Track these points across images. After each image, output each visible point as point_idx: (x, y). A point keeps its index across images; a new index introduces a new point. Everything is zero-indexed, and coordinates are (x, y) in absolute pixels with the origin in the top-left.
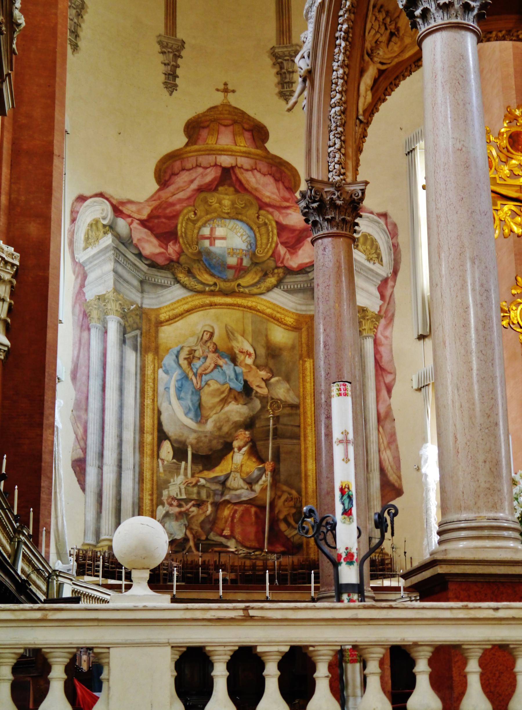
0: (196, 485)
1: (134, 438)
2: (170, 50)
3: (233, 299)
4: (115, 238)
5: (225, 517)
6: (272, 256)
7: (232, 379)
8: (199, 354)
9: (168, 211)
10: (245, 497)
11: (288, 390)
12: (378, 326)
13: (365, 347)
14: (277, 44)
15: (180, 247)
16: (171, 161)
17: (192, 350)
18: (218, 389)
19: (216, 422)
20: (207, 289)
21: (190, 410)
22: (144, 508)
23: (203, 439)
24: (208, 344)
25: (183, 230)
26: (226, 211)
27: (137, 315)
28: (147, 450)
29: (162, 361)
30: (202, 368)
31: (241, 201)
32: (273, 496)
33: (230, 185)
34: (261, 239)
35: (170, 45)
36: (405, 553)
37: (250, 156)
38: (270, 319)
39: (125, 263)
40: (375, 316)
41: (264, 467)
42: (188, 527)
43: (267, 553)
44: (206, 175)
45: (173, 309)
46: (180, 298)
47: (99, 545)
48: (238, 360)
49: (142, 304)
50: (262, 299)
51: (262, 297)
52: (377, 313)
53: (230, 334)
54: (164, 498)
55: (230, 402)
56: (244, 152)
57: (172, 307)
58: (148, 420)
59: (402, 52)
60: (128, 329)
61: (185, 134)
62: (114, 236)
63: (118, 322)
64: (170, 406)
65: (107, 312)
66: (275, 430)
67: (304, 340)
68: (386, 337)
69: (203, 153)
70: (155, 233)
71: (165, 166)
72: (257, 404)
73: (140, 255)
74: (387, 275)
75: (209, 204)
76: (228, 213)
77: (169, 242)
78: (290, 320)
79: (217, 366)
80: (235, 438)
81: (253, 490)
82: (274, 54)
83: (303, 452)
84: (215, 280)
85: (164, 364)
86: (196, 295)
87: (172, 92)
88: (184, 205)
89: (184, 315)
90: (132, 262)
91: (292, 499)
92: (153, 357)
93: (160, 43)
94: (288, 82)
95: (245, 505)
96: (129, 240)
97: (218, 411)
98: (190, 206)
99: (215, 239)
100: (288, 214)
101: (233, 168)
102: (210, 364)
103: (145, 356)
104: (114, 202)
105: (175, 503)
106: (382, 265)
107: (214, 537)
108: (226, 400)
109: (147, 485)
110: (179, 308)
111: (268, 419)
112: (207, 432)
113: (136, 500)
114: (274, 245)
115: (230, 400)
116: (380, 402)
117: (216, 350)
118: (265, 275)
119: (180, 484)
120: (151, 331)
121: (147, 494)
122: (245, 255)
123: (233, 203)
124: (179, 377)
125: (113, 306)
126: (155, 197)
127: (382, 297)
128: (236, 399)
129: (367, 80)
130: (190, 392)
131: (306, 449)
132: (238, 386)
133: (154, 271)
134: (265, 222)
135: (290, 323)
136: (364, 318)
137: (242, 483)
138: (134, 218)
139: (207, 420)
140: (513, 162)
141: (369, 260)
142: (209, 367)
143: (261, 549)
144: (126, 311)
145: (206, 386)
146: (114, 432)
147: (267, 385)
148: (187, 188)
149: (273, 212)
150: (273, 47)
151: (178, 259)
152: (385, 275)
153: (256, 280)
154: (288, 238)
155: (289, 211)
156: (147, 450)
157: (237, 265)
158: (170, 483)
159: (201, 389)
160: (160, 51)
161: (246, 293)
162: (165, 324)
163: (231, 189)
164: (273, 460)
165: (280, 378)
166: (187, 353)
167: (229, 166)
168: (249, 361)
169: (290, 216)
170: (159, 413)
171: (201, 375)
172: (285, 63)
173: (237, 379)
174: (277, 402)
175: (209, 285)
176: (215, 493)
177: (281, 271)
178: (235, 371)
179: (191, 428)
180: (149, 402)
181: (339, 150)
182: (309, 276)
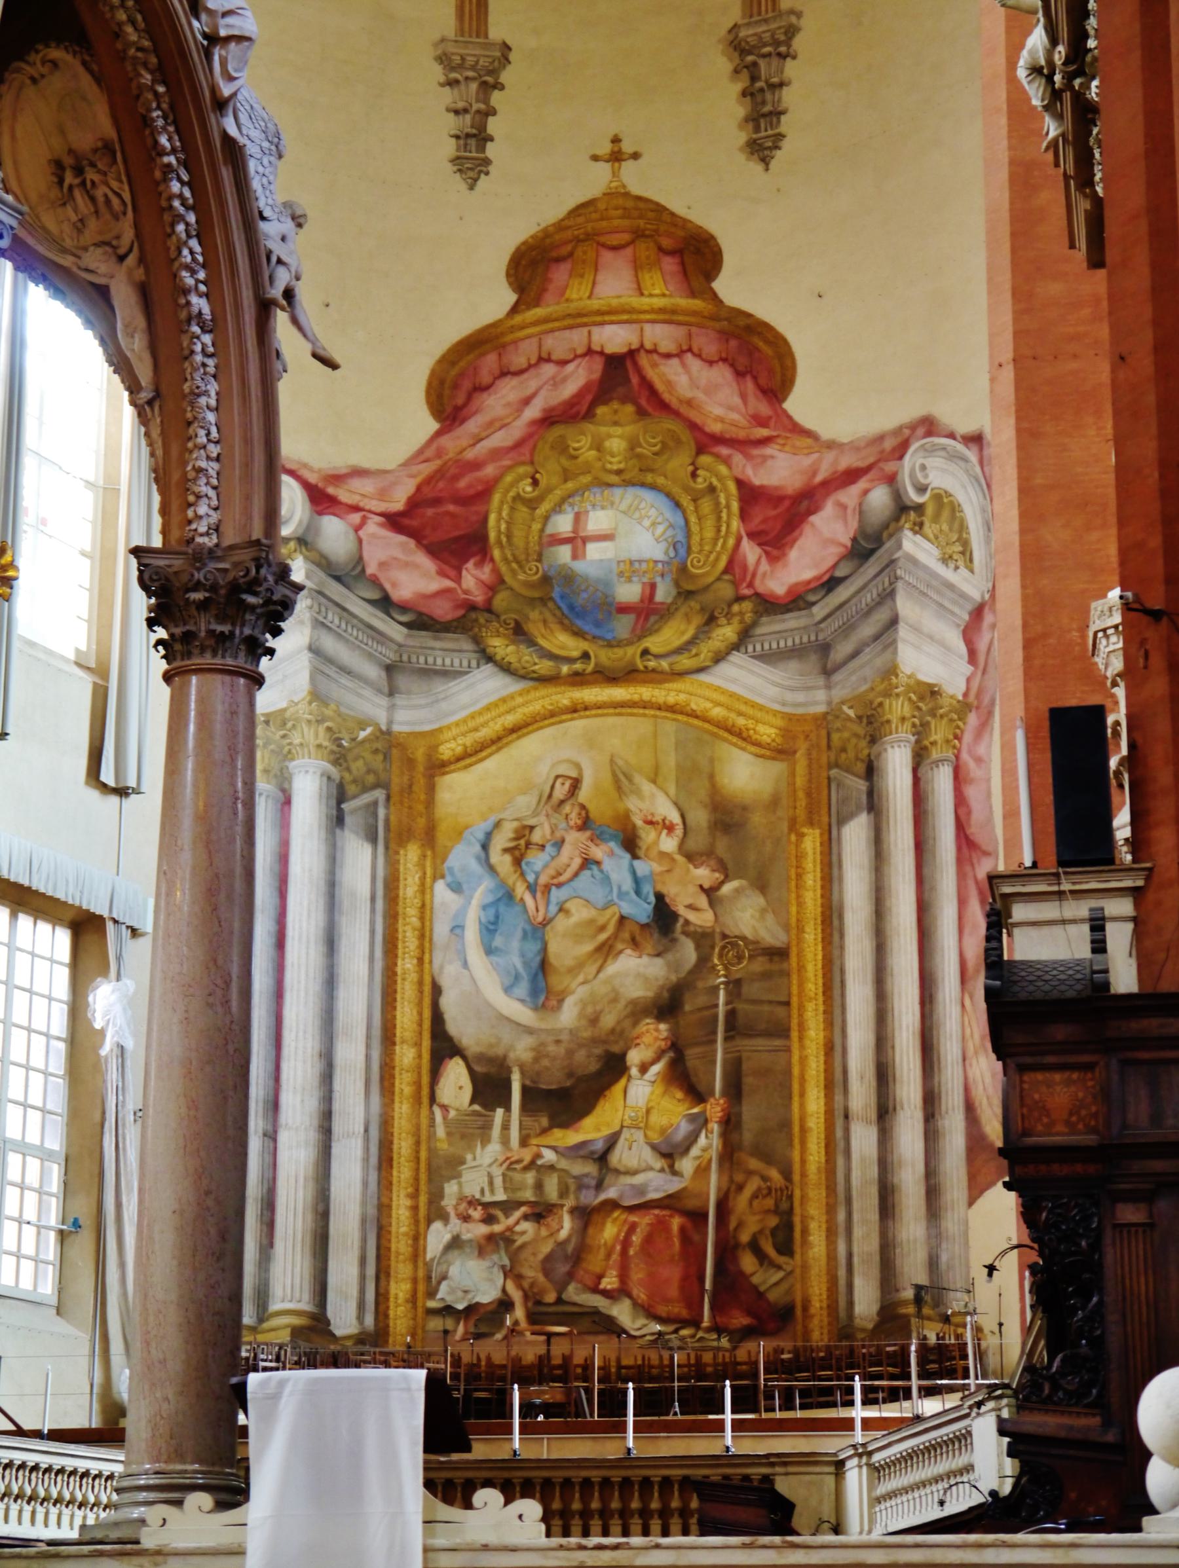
0: (532, 1165)
1: (368, 1057)
2: (471, 74)
3: (632, 690)
4: (314, 568)
5: (605, 1244)
7: (627, 893)
8: (544, 836)
9: (462, 484)
10: (656, 1190)
11: (763, 911)
12: (962, 732)
13: (936, 786)
14: (743, 17)
15: (496, 571)
16: (471, 357)
17: (525, 827)
18: (591, 922)
19: (584, 1004)
20: (565, 669)
21: (517, 977)
22: (394, 1229)
23: (552, 1048)
24: (567, 808)
25: (503, 526)
26: (615, 467)
27: (376, 751)
28: (404, 1084)
29: (443, 862)
30: (552, 872)
31: (654, 438)
32: (725, 1186)
33: (624, 400)
34: (701, 529)
35: (470, 60)
36: (1001, 1325)
37: (675, 318)
38: (722, 733)
39: (343, 626)
40: (957, 706)
41: (704, 1112)
42: (509, 1273)
43: (708, 1330)
44: (564, 380)
45: (476, 730)
46: (493, 698)
47: (266, 1325)
48: (641, 844)
49: (390, 722)
50: (701, 684)
51: (703, 677)
52: (961, 698)
53: (621, 781)
54: (449, 1202)
55: (621, 952)
56: (662, 310)
57: (471, 724)
58: (407, 1009)
60: (351, 789)
61: (510, 284)
62: (313, 562)
63: (322, 775)
64: (465, 972)
65: (289, 752)
66: (731, 1015)
67: (800, 781)
68: (979, 760)
69: (557, 324)
70: (425, 542)
71: (454, 372)
72: (688, 953)
73: (385, 603)
74: (983, 597)
75: (572, 452)
76: (619, 472)
77: (466, 561)
78: (767, 732)
79: (588, 863)
80: (631, 1043)
81: (675, 1173)
82: (738, 46)
83: (796, 1071)
84: (585, 645)
85: (450, 869)
86: (536, 689)
87: (476, 180)
88: (507, 462)
89: (505, 741)
90: (361, 621)
91: (769, 1189)
92: (419, 852)
93: (443, 59)
94: (771, 113)
95: (656, 1212)
96: (354, 568)
97: (590, 977)
98: (523, 463)
99: (585, 540)
100: (765, 458)
101: (632, 354)
102: (572, 859)
103: (397, 853)
104: (312, 478)
105: (477, 1214)
106: (972, 571)
108: (611, 947)
109: (402, 1172)
110: (491, 724)
112: (561, 1031)
113: (372, 1211)
114: (731, 542)
115: (620, 946)
116: (967, 931)
117: (585, 824)
118: (711, 620)
119: (490, 1165)
120: (415, 788)
121: (403, 1193)
122: (662, 575)
123: (633, 444)
124: (490, 899)
125: (309, 735)
126: (429, 453)
128: (635, 943)
131: (803, 1060)
132: (642, 911)
133: (424, 638)
134: (711, 483)
135: (769, 741)
137: (648, 1156)
138: (370, 511)
139: (561, 1001)
141: (946, 560)
142: (569, 866)
143: (696, 1323)
144: (345, 743)
145: (561, 916)
146: (309, 1045)
147: (712, 904)
148: (514, 420)
149: (730, 456)
150: (735, 25)
151: (489, 601)
153: (687, 636)
154: (765, 521)
155: (769, 451)
156: (404, 1084)
157: (642, 601)
158: (463, 1162)
159: (546, 923)
160: (442, 79)
161: (662, 672)
162: (453, 767)
163: (629, 409)
164: (725, 1093)
165: (744, 882)
166: (512, 835)
167: (625, 350)
168: (669, 844)
169: (769, 463)
170: (437, 990)
171: (547, 888)
172: (762, 64)
173: (638, 892)
174: (734, 945)
175: (570, 660)
177: (747, 606)
178: (634, 873)
179: (518, 1024)
180: (408, 966)
182: (812, 615)
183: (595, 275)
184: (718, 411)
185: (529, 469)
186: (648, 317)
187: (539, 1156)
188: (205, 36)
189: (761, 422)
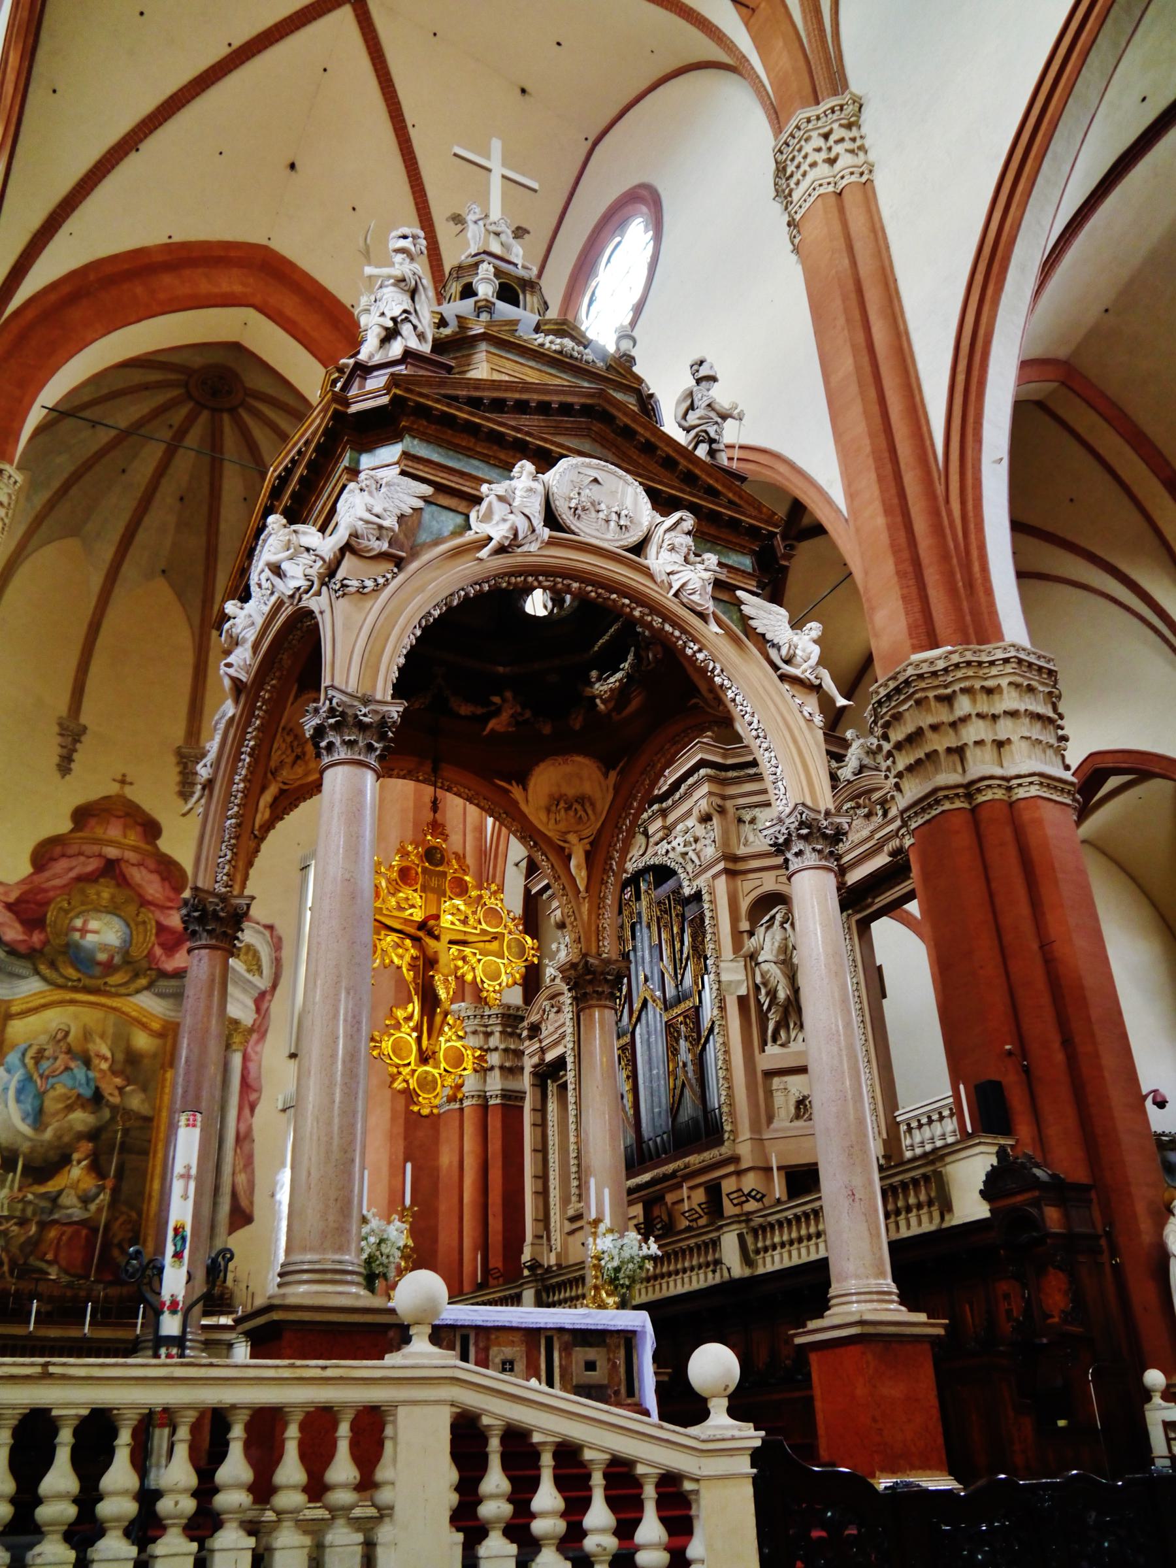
0: (22, 1200)
6: (146, 956)
9: (39, 897)
11: (143, 1101)
15: (47, 936)
18: (65, 1094)
20: (70, 984)
21: (28, 1115)
24: (62, 1044)
33: (112, 878)
51: (131, 999)
53: (87, 1035)
59: (307, 774)
66: (123, 1144)
68: (256, 1053)
72: (107, 1114)
78: (156, 1026)
80: (76, 1150)
81: (87, 1209)
83: (150, 1171)
93: (60, 725)
100: (170, 915)
101: (118, 861)
107: (34, 1262)
111: (116, 1132)
117: (69, 1051)
118: (136, 976)
123: (113, 897)
124: (22, 1078)
127: (258, 1011)
128: (83, 1107)
129: (267, 798)
130: (31, 1095)
131: (154, 1166)
132: (87, 1092)
133: (12, 959)
136: (235, 1030)
139: (46, 1128)
140: (401, 895)
141: (249, 971)
143: (87, 1277)
151: (42, 949)
152: (263, 988)
155: (172, 912)
159: (44, 1093)
163: (113, 882)
164: (115, 1177)
168: (104, 1066)
171: (47, 1077)
172: (190, 764)
176: (43, 1210)
177: (153, 973)
181: (230, 861)
184: (151, 891)
185: (66, 897)
187: (25, 1196)
189: (171, 900)
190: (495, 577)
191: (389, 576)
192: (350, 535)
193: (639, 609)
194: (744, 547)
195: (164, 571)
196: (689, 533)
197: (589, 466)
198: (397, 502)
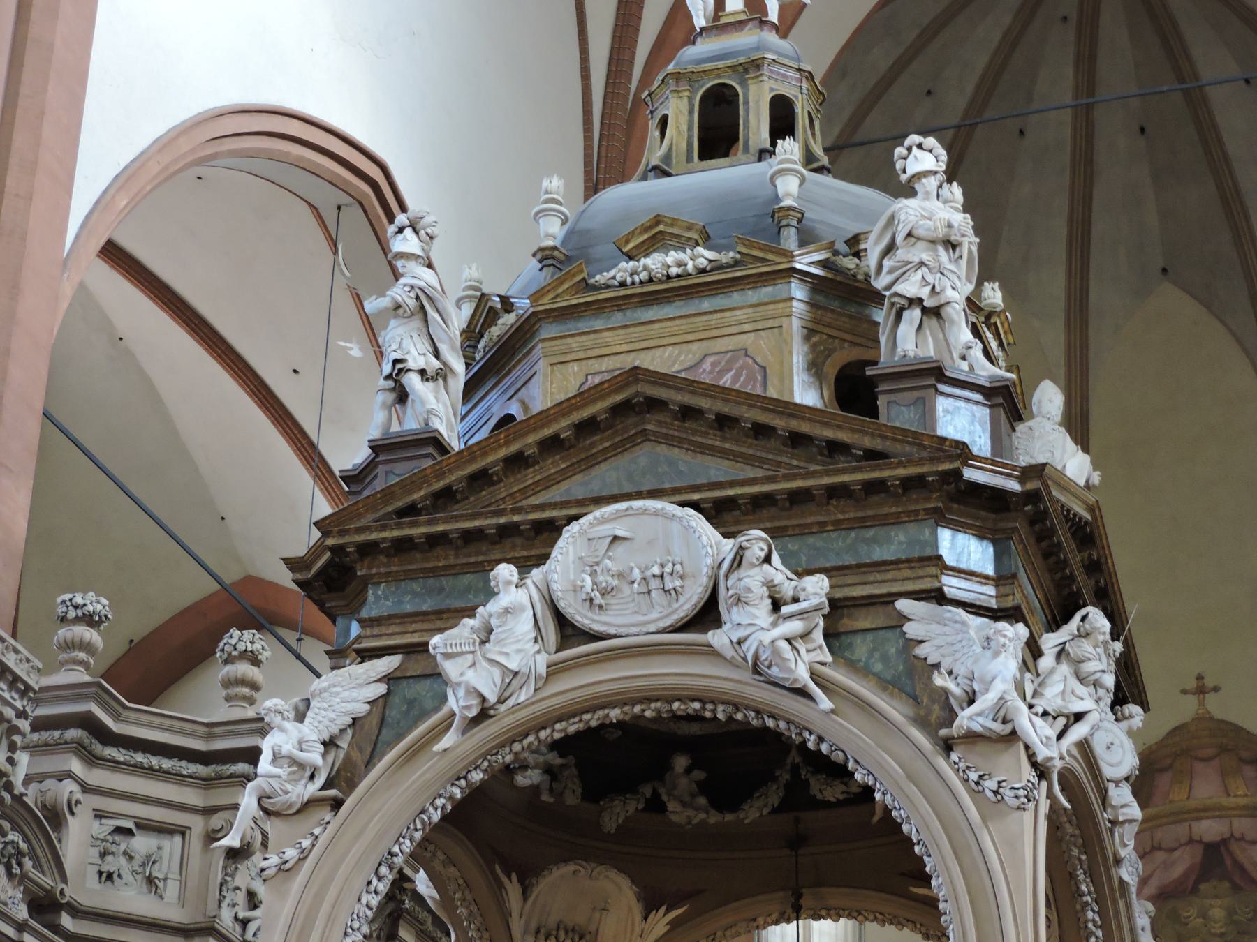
56: (1245, 807)
69: (1164, 820)
75: (1183, 920)
101: (1224, 841)
123: (1231, 912)
167: (1218, 839)
183: (1191, 780)
186: (1235, 812)
188: (1110, 821)
190: (484, 757)
191: (317, 831)
192: (260, 799)
193: (720, 708)
194: (916, 512)
195: (1164, 270)
196: (767, 560)
197: (603, 521)
198: (340, 708)
